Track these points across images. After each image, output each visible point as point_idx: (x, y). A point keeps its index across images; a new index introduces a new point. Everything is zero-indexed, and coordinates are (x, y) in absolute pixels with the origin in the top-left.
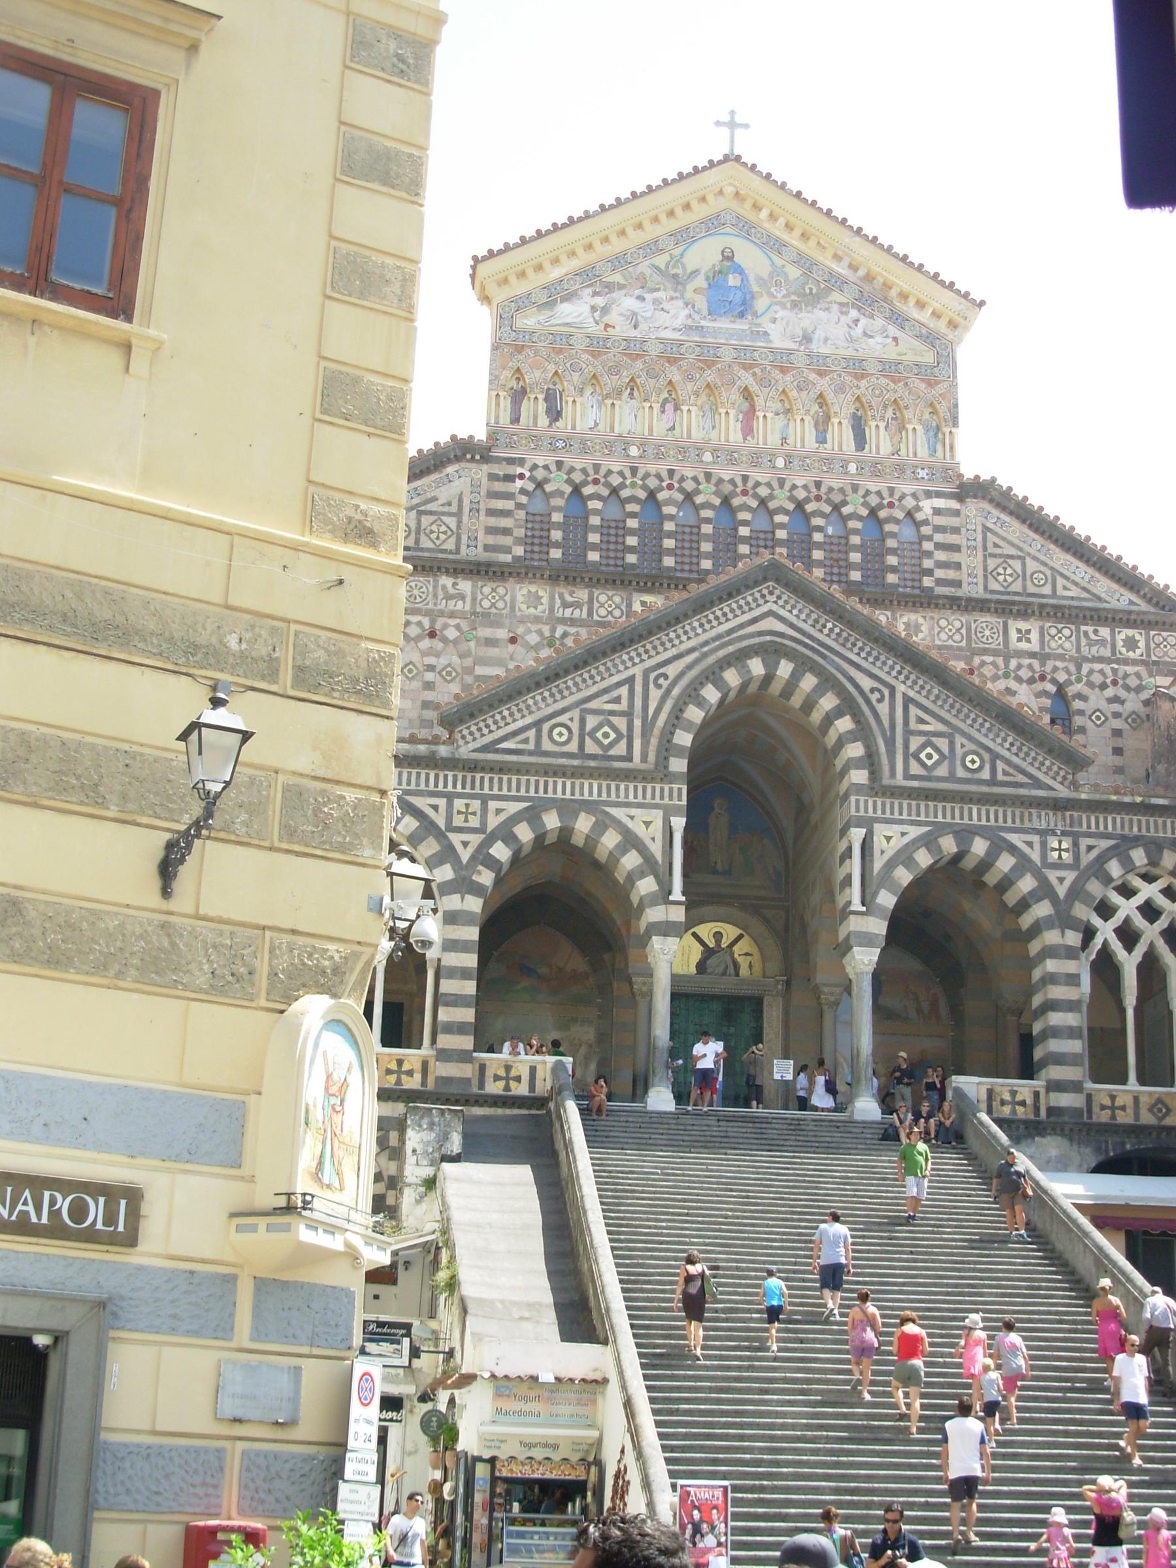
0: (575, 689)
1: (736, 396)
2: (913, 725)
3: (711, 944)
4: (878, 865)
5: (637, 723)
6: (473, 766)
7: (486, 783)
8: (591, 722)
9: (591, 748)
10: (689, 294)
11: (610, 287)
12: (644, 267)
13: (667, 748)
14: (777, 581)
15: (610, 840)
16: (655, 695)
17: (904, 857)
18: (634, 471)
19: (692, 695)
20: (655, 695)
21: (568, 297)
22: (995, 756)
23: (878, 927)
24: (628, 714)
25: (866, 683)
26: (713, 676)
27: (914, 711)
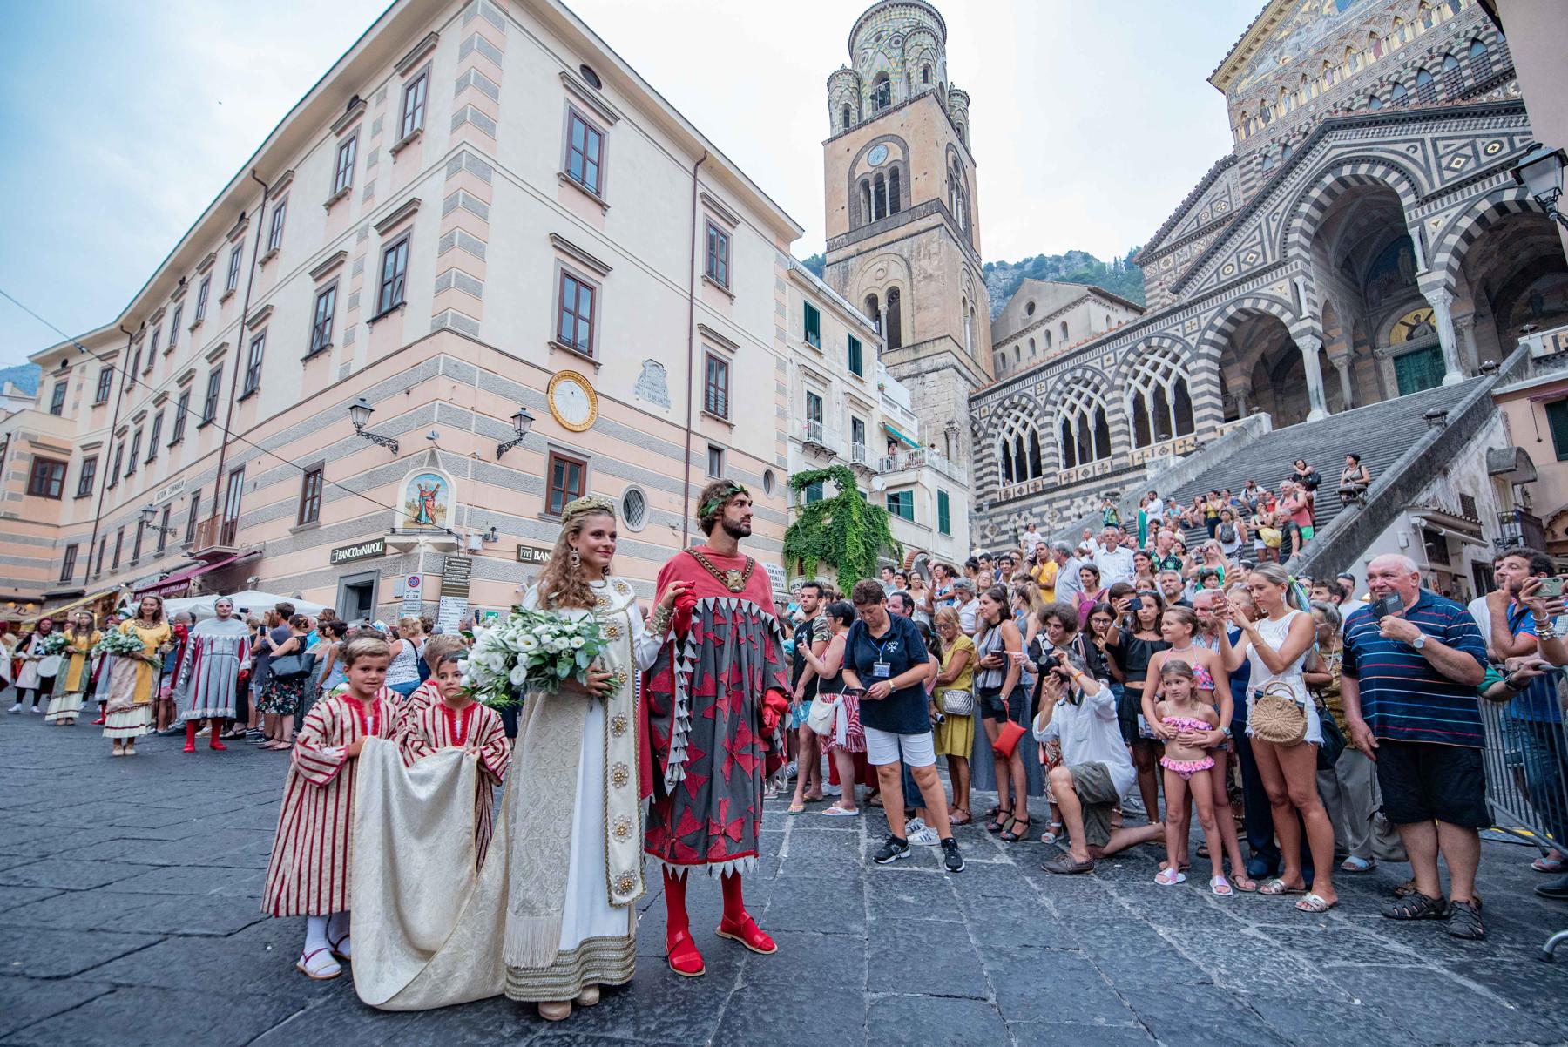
0: (1230, 247)
1: (1365, 41)
2: (1441, 152)
3: (1414, 323)
4: (1431, 241)
5: (1267, 244)
6: (1190, 304)
7: (1197, 309)
8: (1242, 256)
9: (1244, 267)
10: (1326, 11)
11: (1281, 41)
12: (1298, 18)
13: (1285, 246)
14: (1333, 128)
15: (1262, 305)
16: (1273, 225)
17: (1452, 228)
18: (1313, 118)
19: (1294, 213)
20: (1273, 225)
21: (1261, 62)
22: (1510, 136)
23: (1441, 275)
24: (1262, 242)
25: (1402, 148)
26: (1303, 198)
27: (1440, 144)
